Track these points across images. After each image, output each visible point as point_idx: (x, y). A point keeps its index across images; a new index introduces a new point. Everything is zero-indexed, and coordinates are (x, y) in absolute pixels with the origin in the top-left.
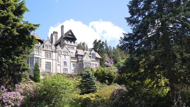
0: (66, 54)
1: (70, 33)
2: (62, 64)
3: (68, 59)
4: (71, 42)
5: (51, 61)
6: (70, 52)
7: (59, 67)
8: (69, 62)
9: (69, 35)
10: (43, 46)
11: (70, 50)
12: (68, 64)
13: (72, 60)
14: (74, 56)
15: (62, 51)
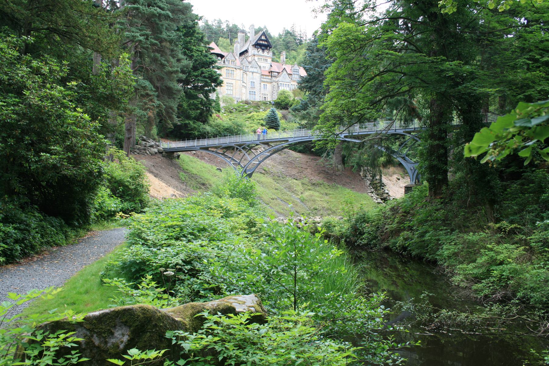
0: (255, 70)
1: (263, 38)
2: (249, 85)
3: (257, 76)
4: (263, 50)
5: (233, 82)
6: (260, 67)
7: (244, 90)
8: (259, 82)
9: (263, 40)
10: (224, 62)
11: (260, 64)
12: (257, 85)
13: (263, 80)
14: (267, 74)
15: (250, 66)
